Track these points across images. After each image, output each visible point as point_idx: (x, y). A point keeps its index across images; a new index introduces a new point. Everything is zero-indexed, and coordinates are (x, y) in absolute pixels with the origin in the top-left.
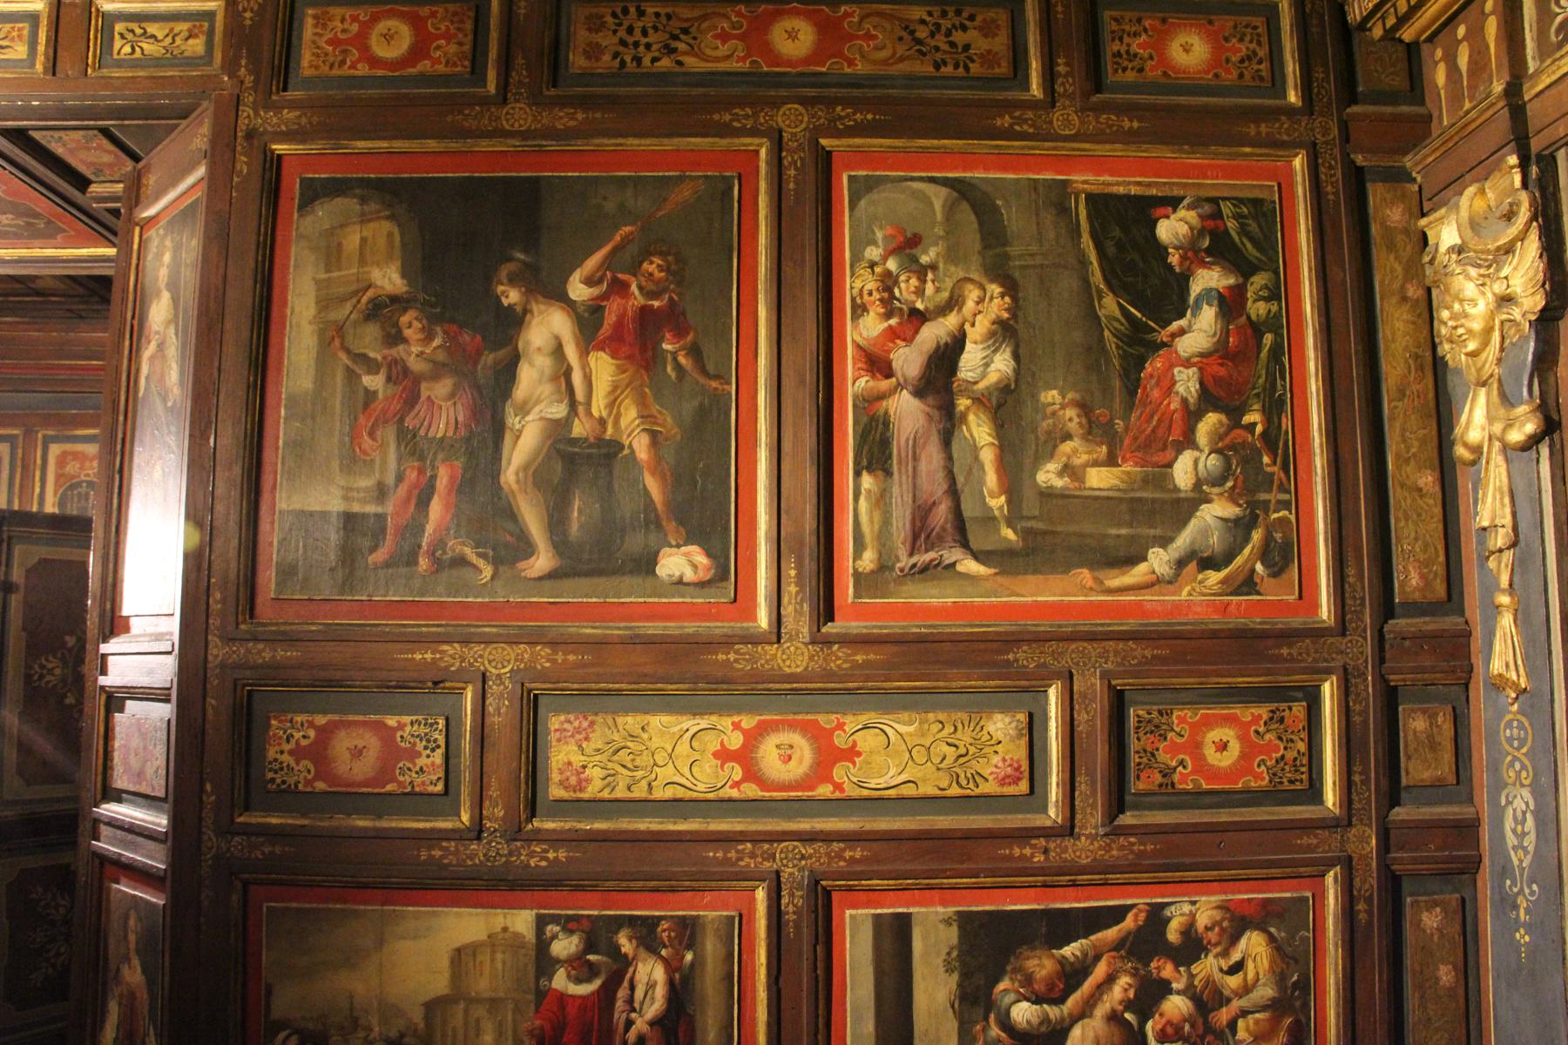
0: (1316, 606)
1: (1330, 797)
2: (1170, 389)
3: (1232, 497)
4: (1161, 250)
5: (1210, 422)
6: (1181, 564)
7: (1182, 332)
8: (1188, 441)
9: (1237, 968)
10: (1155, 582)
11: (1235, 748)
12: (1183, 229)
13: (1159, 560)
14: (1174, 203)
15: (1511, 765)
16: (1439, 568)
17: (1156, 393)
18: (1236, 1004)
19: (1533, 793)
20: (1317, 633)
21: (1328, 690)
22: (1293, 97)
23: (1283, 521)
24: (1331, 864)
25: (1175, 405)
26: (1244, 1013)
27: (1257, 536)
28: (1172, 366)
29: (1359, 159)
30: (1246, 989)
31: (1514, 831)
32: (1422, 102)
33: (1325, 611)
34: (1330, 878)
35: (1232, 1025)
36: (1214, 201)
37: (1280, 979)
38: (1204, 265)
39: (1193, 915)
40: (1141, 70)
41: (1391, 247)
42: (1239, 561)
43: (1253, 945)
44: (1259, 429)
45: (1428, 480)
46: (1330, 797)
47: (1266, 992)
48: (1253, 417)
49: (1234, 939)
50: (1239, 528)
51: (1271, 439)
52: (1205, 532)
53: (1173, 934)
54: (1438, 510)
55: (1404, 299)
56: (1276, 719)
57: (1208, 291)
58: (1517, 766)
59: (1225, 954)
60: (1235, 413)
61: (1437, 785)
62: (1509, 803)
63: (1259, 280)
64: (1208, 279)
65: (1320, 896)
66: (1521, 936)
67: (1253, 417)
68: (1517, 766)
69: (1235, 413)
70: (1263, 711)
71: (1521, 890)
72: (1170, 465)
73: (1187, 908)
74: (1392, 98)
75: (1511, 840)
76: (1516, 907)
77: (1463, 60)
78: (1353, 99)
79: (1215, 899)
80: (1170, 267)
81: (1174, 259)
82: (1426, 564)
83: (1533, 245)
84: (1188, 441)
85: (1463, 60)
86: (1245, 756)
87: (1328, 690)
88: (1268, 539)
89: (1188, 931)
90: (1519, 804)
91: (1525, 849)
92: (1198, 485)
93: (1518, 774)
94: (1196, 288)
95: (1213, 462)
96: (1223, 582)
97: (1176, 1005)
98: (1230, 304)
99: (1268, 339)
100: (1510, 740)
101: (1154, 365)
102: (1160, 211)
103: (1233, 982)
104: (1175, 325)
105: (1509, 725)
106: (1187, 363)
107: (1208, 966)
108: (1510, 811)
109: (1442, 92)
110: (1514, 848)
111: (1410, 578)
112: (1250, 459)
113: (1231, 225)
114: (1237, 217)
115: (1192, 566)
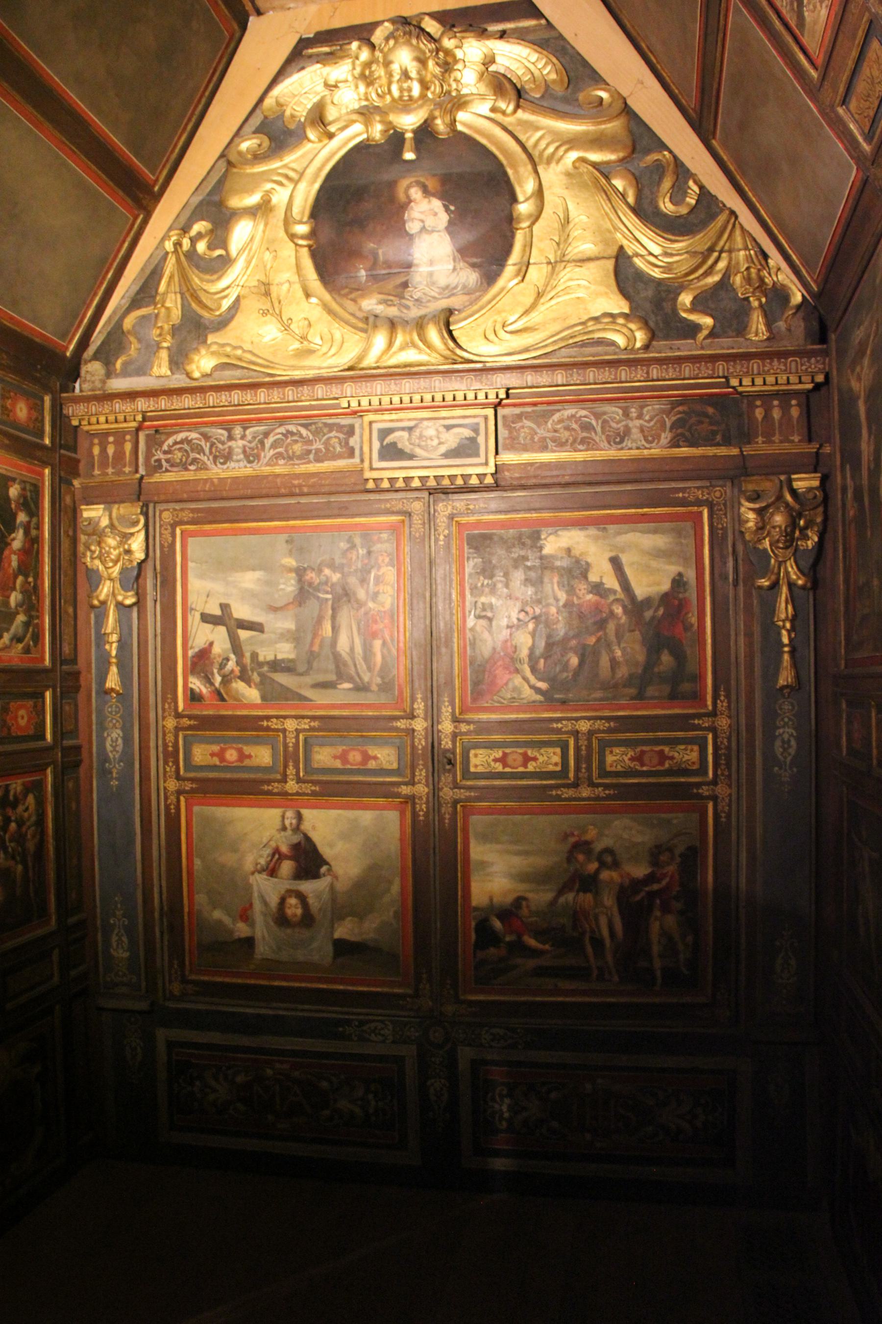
0: (43, 659)
1: (49, 736)
2: (10, 565)
3: (26, 615)
4: (8, 499)
5: (20, 579)
6: (12, 640)
7: (14, 539)
8: (14, 589)
9: (27, 809)
10: (6, 648)
11: (26, 719)
12: (16, 493)
13: (6, 637)
14: (14, 480)
15: (111, 721)
16: (72, 646)
17: (6, 565)
18: (28, 824)
19: (123, 731)
20: (46, 671)
21: (48, 695)
22: (47, 441)
23: (37, 624)
24: (48, 765)
25: (11, 571)
26: (29, 828)
27: (31, 630)
28: (10, 554)
29: (62, 474)
30: (30, 816)
31: (111, 745)
32: (76, 452)
33: (47, 662)
34: (49, 771)
35: (26, 832)
36: (24, 482)
37: (37, 810)
38: (21, 510)
39: (15, 789)
40: (8, 416)
41: (66, 512)
42: (26, 639)
43: (31, 799)
44: (32, 584)
45: (71, 610)
46: (49, 736)
47: (34, 818)
48: (31, 579)
49: (26, 796)
50: (27, 624)
51: (35, 588)
52: (17, 627)
53: (11, 798)
54: (72, 623)
55: (68, 536)
56: (35, 706)
57: (22, 522)
58: (114, 721)
59: (24, 804)
60: (26, 576)
61: (71, 732)
62: (108, 735)
63: (34, 520)
64: (22, 517)
65: (46, 776)
66: (114, 783)
67: (31, 579)
68: (114, 721)
69: (26, 576)
70: (30, 703)
71: (114, 766)
72: (9, 597)
73: (14, 785)
74: (68, 448)
75: (109, 748)
76: (111, 773)
77: (111, 450)
78: (61, 447)
79: (19, 781)
80: (11, 509)
81: (13, 506)
82: (69, 644)
83: (143, 533)
84: (14, 589)
85: (111, 450)
86: (28, 721)
87: (48, 695)
88: (33, 631)
89: (15, 795)
90: (114, 735)
91: (117, 752)
92: (16, 606)
93: (114, 725)
94: (18, 521)
95: (20, 597)
96: (23, 648)
97: (13, 825)
98: (27, 528)
99: (36, 546)
100: (111, 713)
101: (6, 552)
102: (10, 483)
103: (26, 814)
104: (13, 535)
105: (111, 707)
106: (15, 553)
107: (21, 808)
108: (109, 738)
109: (96, 458)
110: (111, 752)
111: (67, 649)
112: (30, 599)
113: (29, 494)
114: (31, 491)
115: (15, 641)
